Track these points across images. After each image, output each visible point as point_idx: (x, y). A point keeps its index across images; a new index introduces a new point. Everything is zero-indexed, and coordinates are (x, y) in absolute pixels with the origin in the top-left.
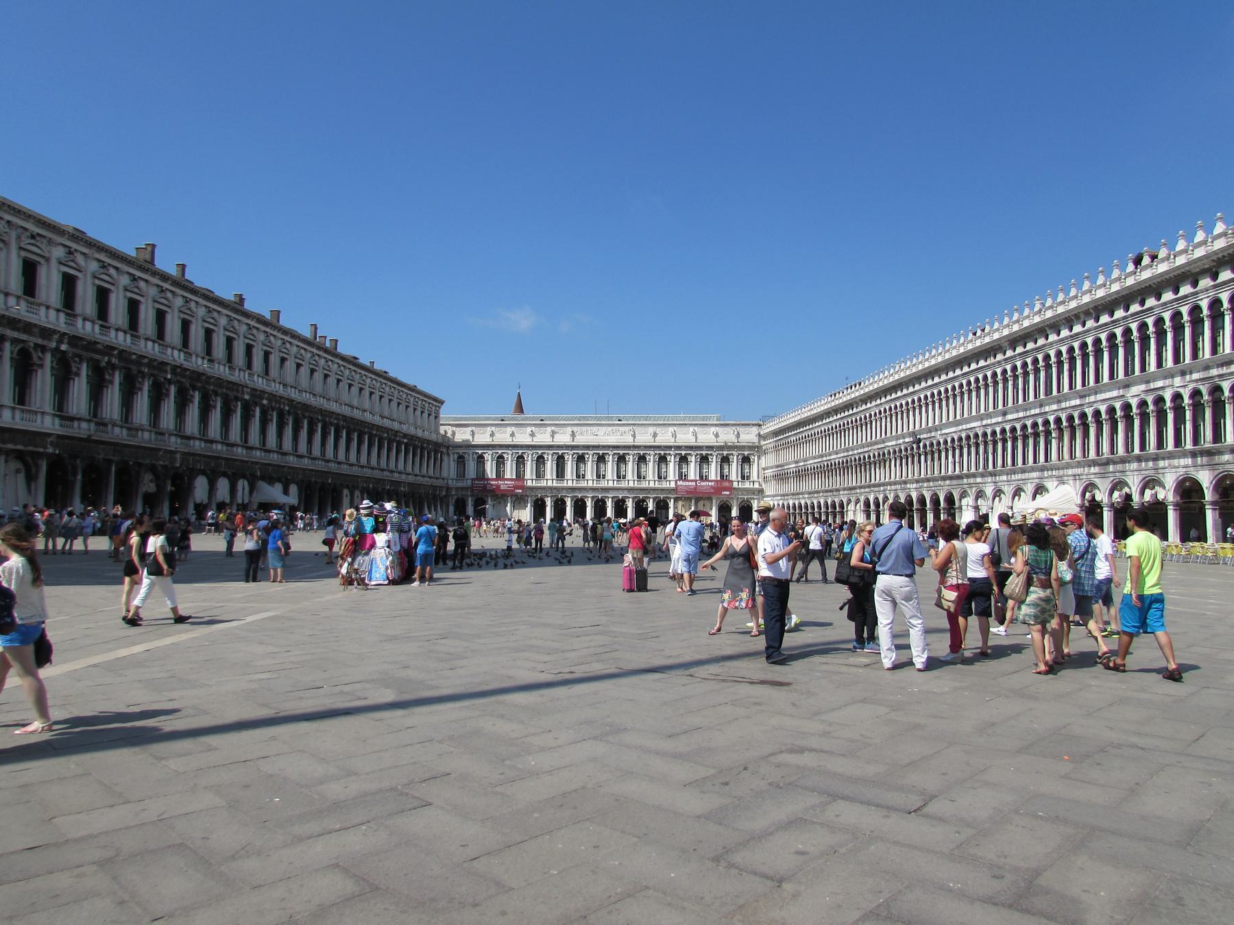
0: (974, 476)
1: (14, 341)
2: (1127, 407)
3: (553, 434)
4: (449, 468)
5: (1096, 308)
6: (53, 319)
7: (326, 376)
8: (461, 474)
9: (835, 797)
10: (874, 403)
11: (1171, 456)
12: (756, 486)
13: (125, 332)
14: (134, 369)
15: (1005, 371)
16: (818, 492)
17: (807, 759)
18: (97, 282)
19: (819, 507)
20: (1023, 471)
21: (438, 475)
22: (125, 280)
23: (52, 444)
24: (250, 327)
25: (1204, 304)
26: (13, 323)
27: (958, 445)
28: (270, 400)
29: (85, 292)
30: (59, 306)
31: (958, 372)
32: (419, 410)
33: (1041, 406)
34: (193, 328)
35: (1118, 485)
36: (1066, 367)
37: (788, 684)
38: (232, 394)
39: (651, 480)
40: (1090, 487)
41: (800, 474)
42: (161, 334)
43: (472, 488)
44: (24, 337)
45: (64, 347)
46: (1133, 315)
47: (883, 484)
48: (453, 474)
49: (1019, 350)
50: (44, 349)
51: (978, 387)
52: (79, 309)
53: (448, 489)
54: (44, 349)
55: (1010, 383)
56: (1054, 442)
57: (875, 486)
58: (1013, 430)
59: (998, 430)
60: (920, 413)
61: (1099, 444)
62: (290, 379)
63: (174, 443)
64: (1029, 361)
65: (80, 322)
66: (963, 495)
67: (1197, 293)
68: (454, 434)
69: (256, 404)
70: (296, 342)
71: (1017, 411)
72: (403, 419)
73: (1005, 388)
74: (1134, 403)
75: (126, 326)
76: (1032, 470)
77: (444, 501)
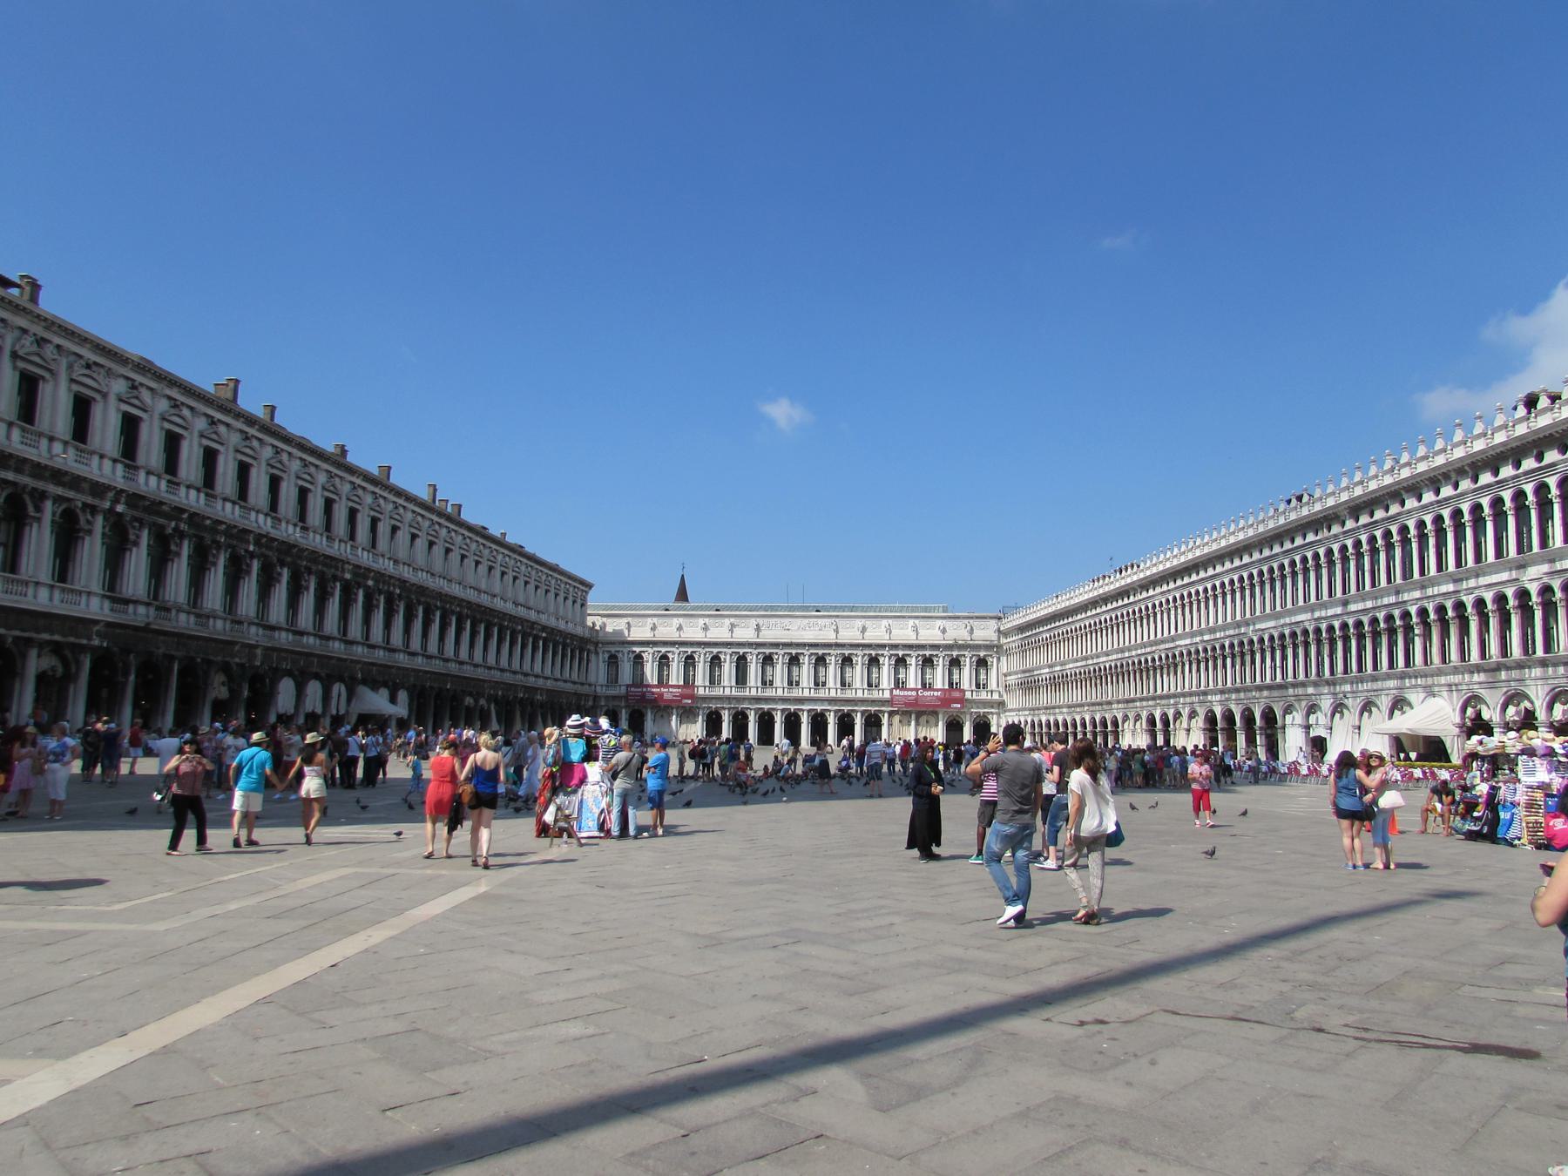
0: (1303, 685)
1: (58, 499)
2: (1523, 595)
4: (598, 671)
6: (110, 473)
7: (448, 551)
8: (613, 679)
10: (1158, 590)
12: (996, 696)
13: (199, 490)
15: (1344, 548)
16: (1082, 705)
18: (167, 426)
19: (1084, 725)
20: (1374, 679)
21: (583, 679)
23: (99, 634)
24: (354, 486)
26: (58, 476)
27: (1280, 644)
28: (377, 581)
29: (151, 433)
30: (116, 455)
31: (1277, 549)
32: (562, 595)
33: (1397, 593)
34: (284, 486)
36: (1432, 541)
38: (329, 572)
39: (858, 689)
40: (1473, 700)
41: (1057, 682)
42: (243, 493)
43: (626, 697)
44: (70, 494)
45: (120, 508)
46: (1526, 473)
47: (1174, 696)
48: (602, 679)
49: (1364, 519)
50: (94, 510)
52: (141, 458)
53: (596, 698)
54: (94, 510)
55: (1352, 564)
56: (1418, 642)
57: (1161, 697)
58: (1359, 624)
59: (1337, 624)
60: (1224, 603)
62: (402, 554)
63: (254, 634)
64: (1378, 534)
65: (142, 476)
66: (1288, 710)
69: (359, 585)
70: (411, 506)
71: (1364, 600)
72: (541, 607)
73: (1345, 570)
74: (1533, 589)
75: (200, 483)
76: (1388, 677)
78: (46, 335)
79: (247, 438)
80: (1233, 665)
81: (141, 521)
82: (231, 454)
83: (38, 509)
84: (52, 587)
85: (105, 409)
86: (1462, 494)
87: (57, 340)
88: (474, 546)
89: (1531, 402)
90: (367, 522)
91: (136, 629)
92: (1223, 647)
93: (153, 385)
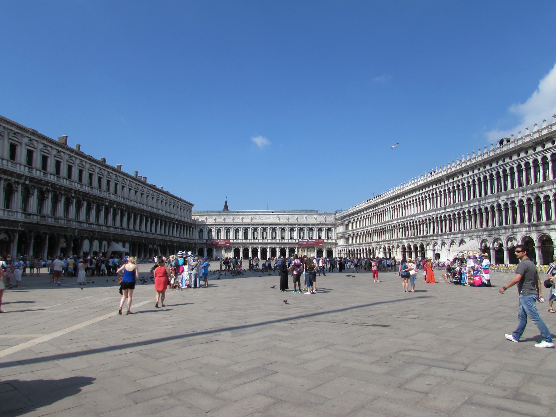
0: (432, 236)
1: (6, 180)
4: (196, 235)
6: (23, 170)
7: (142, 194)
8: (201, 238)
9: (431, 366)
10: (387, 204)
11: (519, 227)
12: (334, 241)
13: (54, 175)
15: (445, 190)
16: (362, 244)
17: (412, 353)
18: (42, 153)
19: (363, 251)
20: (454, 234)
21: (191, 238)
22: (54, 152)
23: (21, 226)
24: (109, 173)
25: (531, 161)
26: (5, 172)
28: (117, 205)
31: (424, 190)
32: (183, 209)
33: (461, 205)
34: (84, 173)
36: (472, 188)
37: (389, 326)
38: (101, 203)
39: (287, 239)
40: (484, 241)
41: (354, 236)
43: (206, 244)
45: (27, 182)
46: (500, 166)
48: (198, 238)
49: (451, 181)
50: (18, 183)
51: (433, 197)
52: (34, 165)
53: (195, 244)
54: (18, 183)
55: (447, 195)
56: (468, 221)
57: (388, 241)
58: (449, 216)
59: (443, 216)
62: (126, 195)
63: (75, 225)
64: (455, 185)
65: (34, 171)
67: (527, 156)
69: (111, 207)
70: (129, 179)
73: (445, 198)
74: (502, 204)
75: (54, 172)
76: (458, 233)
80: (411, 230)
81: (34, 186)
82: (65, 163)
85: (21, 148)
88: (151, 192)
89: (501, 142)
90: (114, 185)
91: (33, 224)
92: (407, 224)
93: (37, 139)
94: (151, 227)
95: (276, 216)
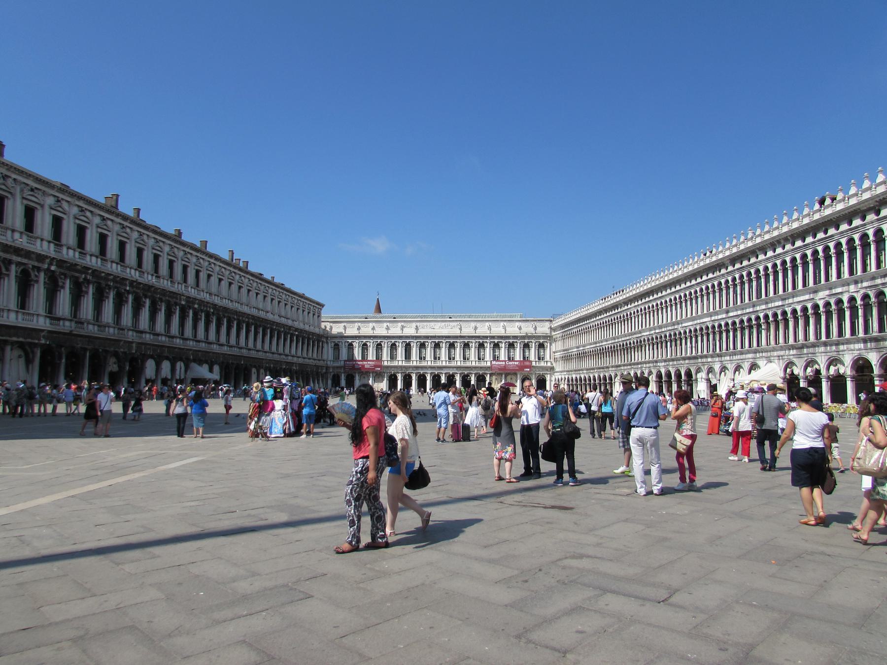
0: (706, 357)
1: (18, 264)
2: (816, 307)
3: (403, 328)
4: (328, 353)
5: (792, 236)
7: (240, 287)
8: (337, 357)
9: (605, 591)
10: (633, 305)
11: (848, 342)
12: (549, 364)
13: (97, 257)
14: (103, 283)
15: (727, 281)
16: (593, 369)
17: (584, 563)
18: (78, 222)
20: (741, 353)
22: (97, 220)
23: (44, 337)
24: (185, 253)
25: (871, 233)
26: (18, 251)
27: (694, 335)
28: (200, 305)
30: (50, 239)
31: (693, 282)
32: (307, 311)
33: (754, 306)
34: (145, 253)
35: (810, 363)
36: (771, 278)
37: (571, 509)
38: (173, 301)
39: (473, 361)
40: (790, 364)
41: (581, 356)
42: (122, 258)
43: (344, 367)
44: (25, 261)
45: (53, 268)
46: (819, 240)
47: (641, 363)
48: (331, 357)
49: (738, 266)
50: (39, 269)
52: (64, 240)
53: (327, 368)
54: (39, 269)
55: (731, 290)
56: (764, 332)
57: (634, 364)
58: (734, 323)
59: (723, 323)
60: (667, 312)
61: (796, 333)
62: (214, 290)
63: (131, 336)
64: (744, 274)
65: (65, 250)
66: (698, 370)
67: (865, 225)
68: (331, 328)
70: (218, 263)
71: (737, 310)
73: (728, 294)
74: (821, 304)
75: (97, 252)
76: (748, 352)
77: (324, 376)
78: (8, 174)
79: (123, 227)
80: (671, 346)
82: (115, 237)
83: (8, 269)
84: (17, 312)
85: (43, 213)
86: (787, 252)
87: (14, 176)
91: (64, 334)
92: (666, 336)
93: (69, 199)
94: (255, 340)
95: (455, 324)
